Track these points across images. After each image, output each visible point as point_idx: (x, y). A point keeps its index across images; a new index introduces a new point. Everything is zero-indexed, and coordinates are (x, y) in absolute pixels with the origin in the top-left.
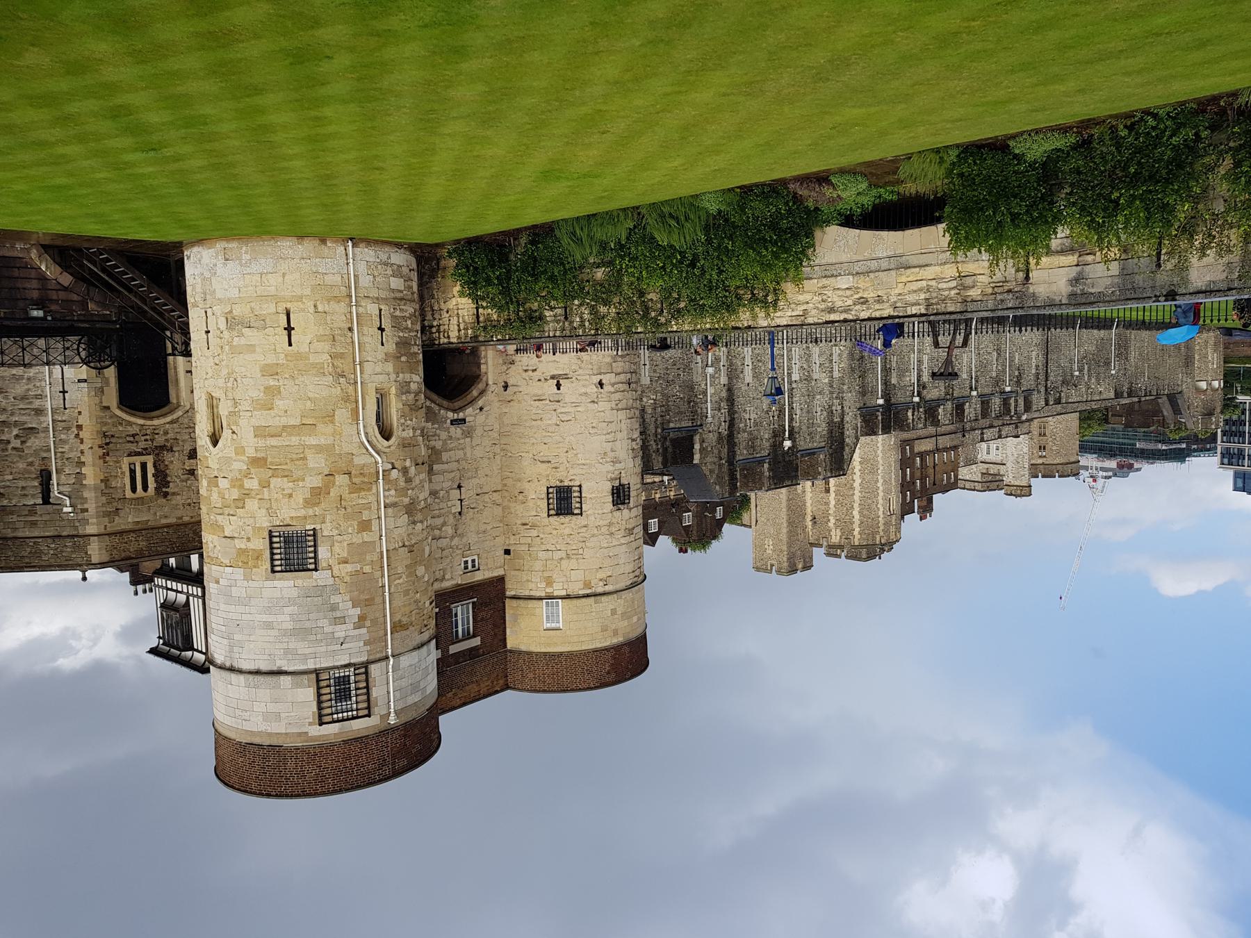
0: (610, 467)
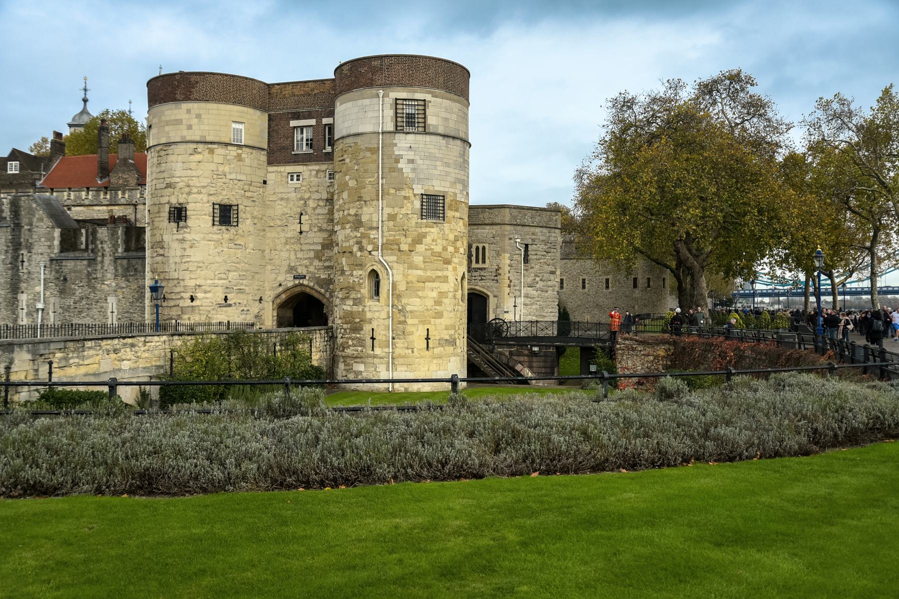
0: (188, 237)
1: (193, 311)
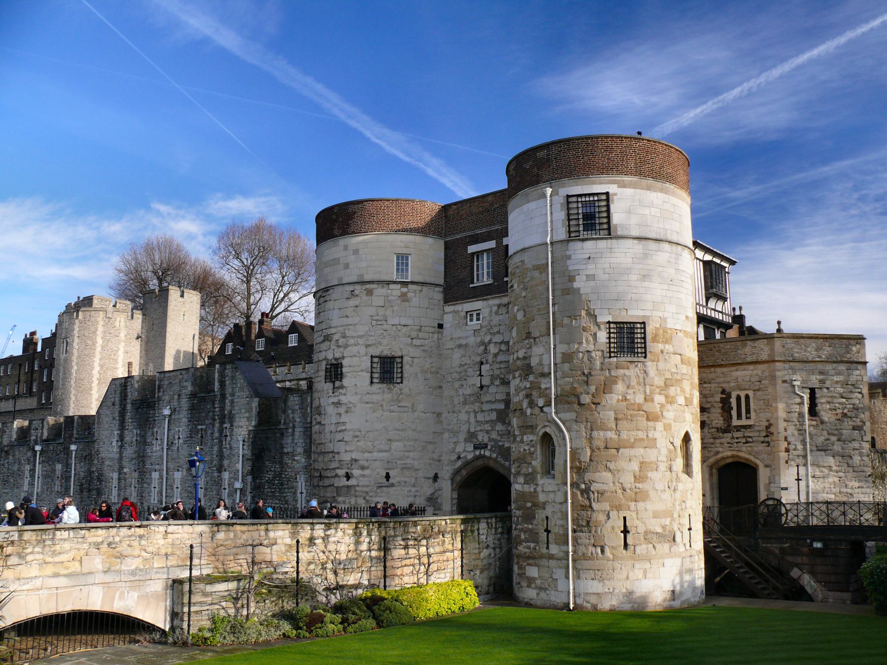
0: (343, 399)
1: (348, 491)
